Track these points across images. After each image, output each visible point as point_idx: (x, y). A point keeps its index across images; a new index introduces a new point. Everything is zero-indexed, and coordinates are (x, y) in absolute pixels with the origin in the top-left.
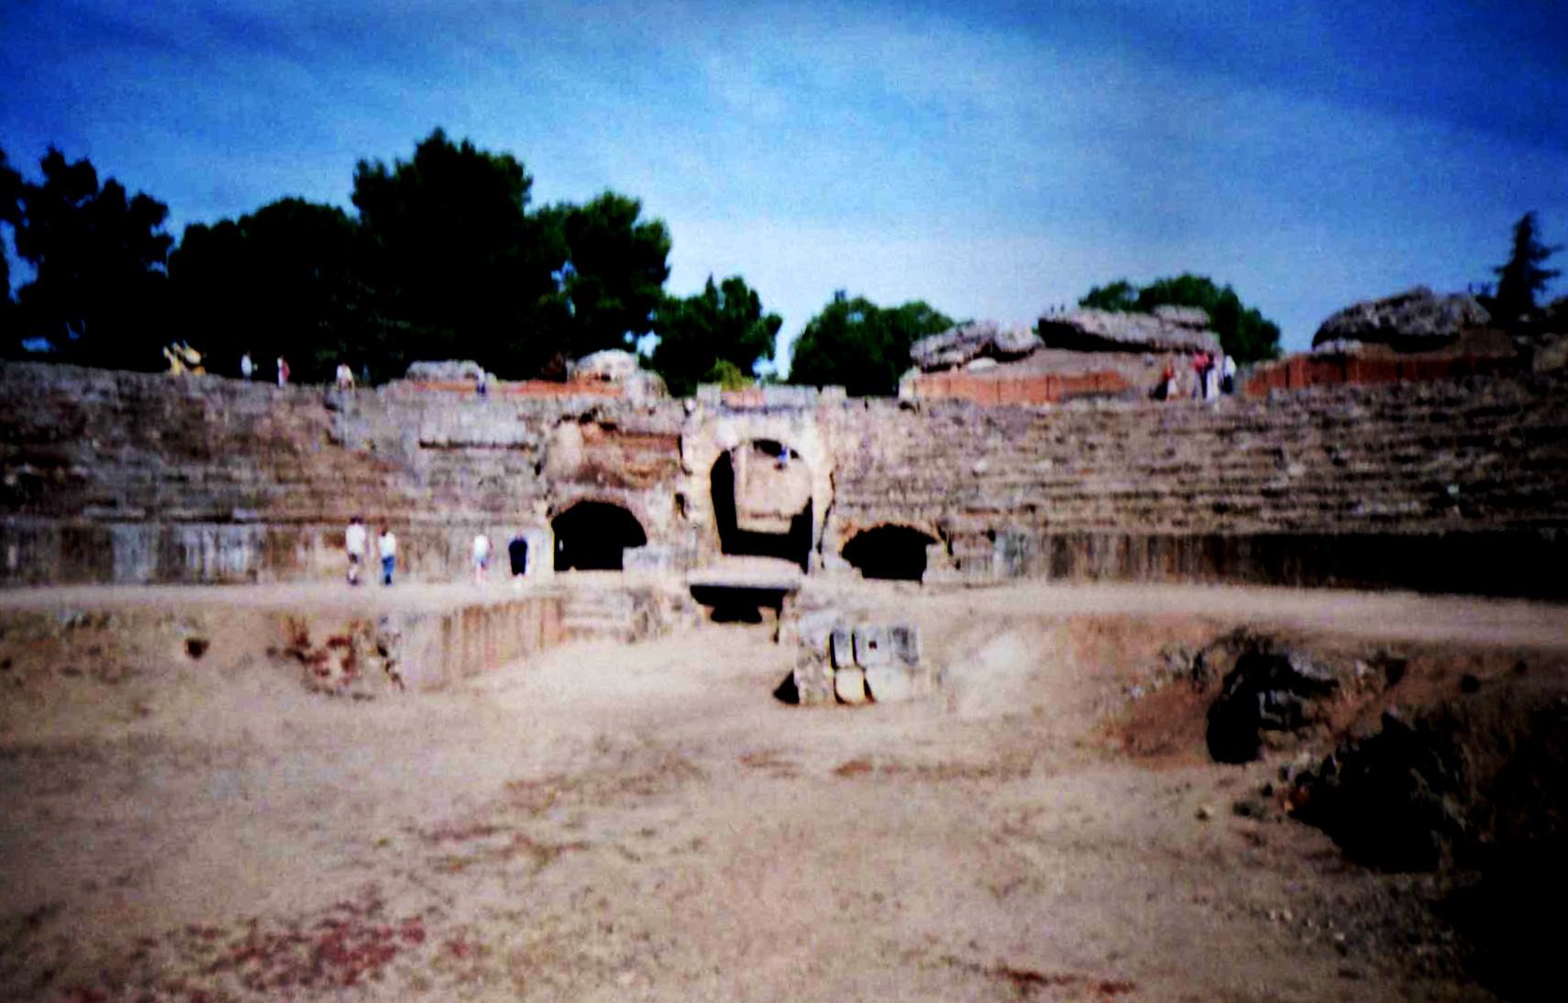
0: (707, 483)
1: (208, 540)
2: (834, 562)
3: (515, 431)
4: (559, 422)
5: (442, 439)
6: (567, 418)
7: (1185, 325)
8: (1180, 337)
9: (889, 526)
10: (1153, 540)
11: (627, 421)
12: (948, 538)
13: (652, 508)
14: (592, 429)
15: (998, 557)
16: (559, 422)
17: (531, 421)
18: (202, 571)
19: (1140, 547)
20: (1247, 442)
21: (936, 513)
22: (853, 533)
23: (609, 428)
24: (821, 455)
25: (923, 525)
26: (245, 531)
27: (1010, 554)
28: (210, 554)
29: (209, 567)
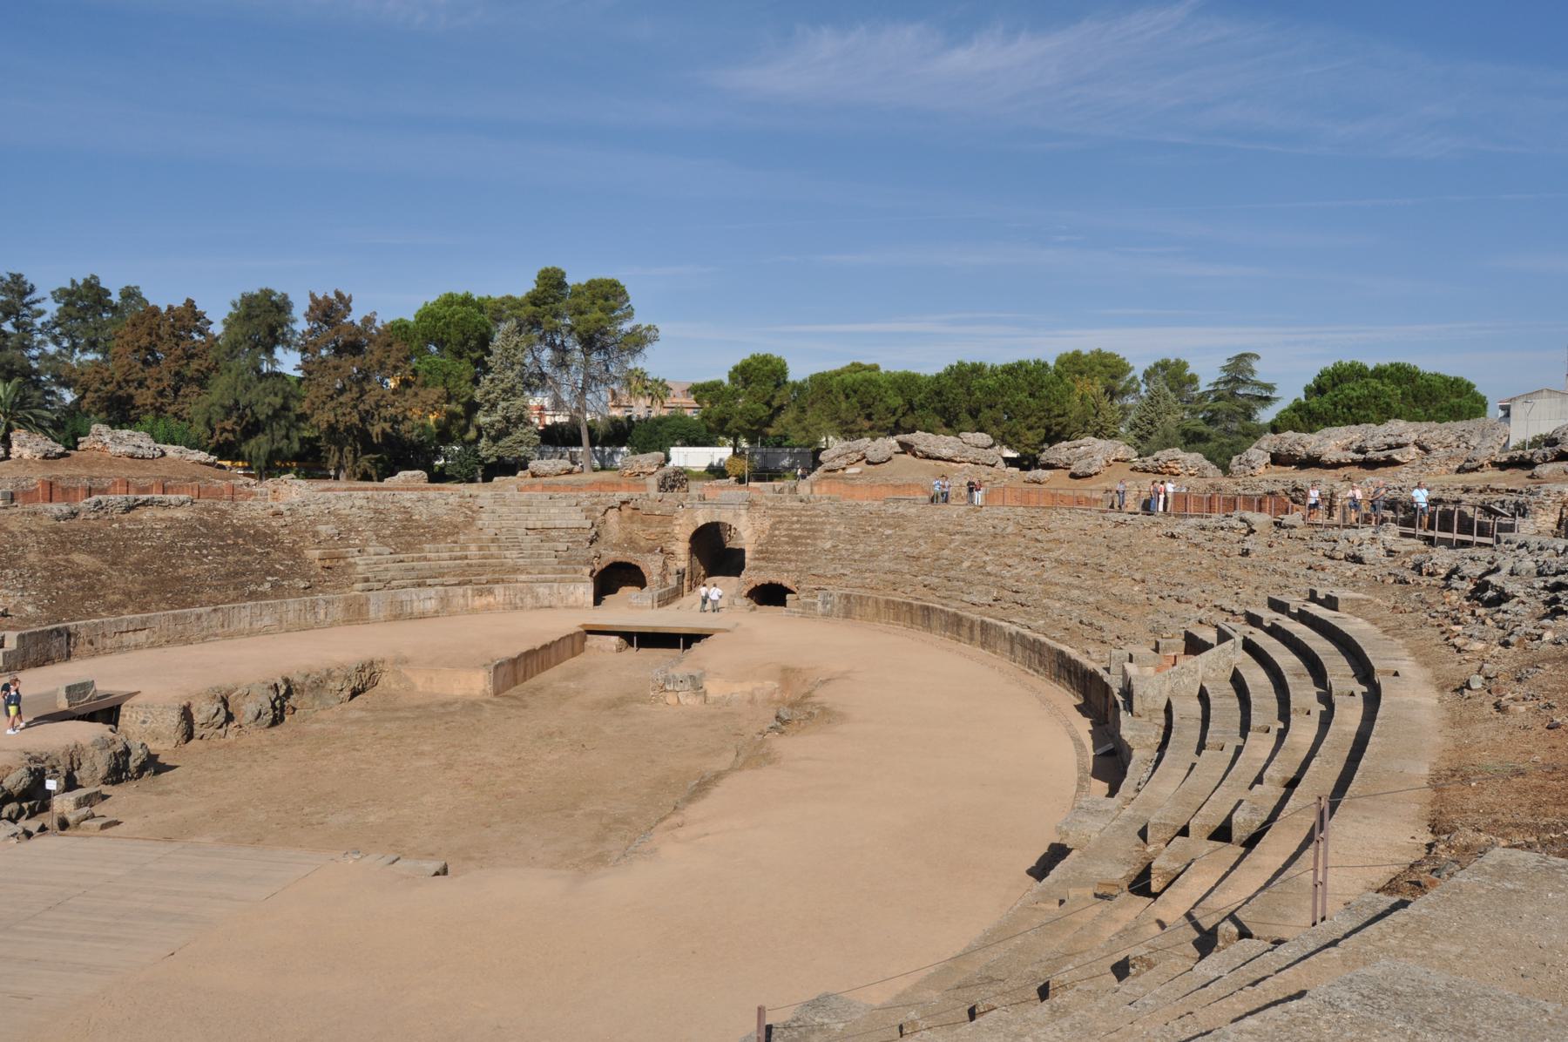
0: (687, 545)
1: (414, 597)
3: (577, 519)
4: (607, 510)
5: (539, 525)
6: (612, 507)
8: (972, 454)
9: (771, 584)
10: (887, 602)
11: (646, 506)
13: (651, 566)
14: (627, 511)
15: (820, 604)
16: (607, 510)
17: (589, 511)
18: (412, 613)
19: (882, 605)
21: (794, 576)
22: (753, 586)
24: (749, 531)
25: (787, 583)
26: (432, 592)
27: (825, 603)
28: (415, 604)
29: (415, 610)
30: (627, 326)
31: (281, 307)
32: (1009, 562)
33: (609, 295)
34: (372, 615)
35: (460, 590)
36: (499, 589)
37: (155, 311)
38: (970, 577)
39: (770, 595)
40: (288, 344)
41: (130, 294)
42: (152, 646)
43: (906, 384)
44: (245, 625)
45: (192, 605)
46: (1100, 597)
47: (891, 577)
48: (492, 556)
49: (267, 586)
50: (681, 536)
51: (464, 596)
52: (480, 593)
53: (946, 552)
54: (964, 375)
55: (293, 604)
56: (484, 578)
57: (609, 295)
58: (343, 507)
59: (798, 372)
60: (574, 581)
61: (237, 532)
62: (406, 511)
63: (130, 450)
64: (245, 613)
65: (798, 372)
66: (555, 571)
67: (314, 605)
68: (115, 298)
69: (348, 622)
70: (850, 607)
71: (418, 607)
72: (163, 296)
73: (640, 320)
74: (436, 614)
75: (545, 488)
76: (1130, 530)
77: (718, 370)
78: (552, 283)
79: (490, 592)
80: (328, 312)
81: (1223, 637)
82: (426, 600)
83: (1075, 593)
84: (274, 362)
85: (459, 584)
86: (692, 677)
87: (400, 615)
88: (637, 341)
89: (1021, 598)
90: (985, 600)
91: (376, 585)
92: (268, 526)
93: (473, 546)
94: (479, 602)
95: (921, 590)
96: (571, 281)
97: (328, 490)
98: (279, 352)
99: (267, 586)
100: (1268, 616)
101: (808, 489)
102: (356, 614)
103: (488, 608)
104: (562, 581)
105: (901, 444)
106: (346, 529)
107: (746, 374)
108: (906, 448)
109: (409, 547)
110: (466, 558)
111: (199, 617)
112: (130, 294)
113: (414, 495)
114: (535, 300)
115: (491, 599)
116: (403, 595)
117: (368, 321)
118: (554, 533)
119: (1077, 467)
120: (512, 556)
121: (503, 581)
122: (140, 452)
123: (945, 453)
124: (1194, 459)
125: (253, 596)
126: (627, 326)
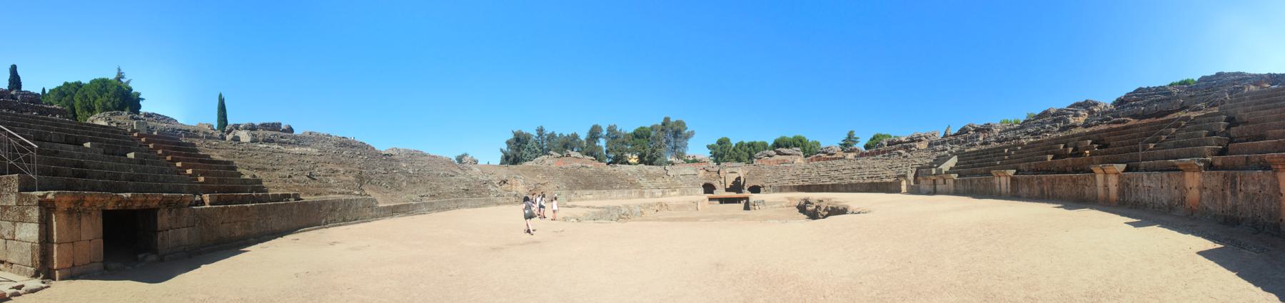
2: (746, 191)
3: (693, 172)
8: (796, 153)
12: (763, 187)
17: (696, 170)
20: (807, 170)
23: (707, 171)
33: (679, 123)
35: (667, 190)
36: (678, 190)
40: (601, 137)
42: (593, 199)
49: (618, 187)
52: (673, 191)
55: (626, 191)
59: (734, 142)
65: (734, 142)
67: (631, 193)
68: (558, 136)
69: (639, 198)
74: (662, 196)
78: (667, 120)
80: (611, 129)
84: (599, 142)
86: (763, 201)
94: (672, 193)
96: (671, 120)
98: (601, 139)
102: (642, 195)
103: (675, 196)
106: (634, 174)
107: (721, 142)
108: (779, 153)
115: (675, 193)
116: (653, 191)
117: (621, 130)
126: (686, 131)
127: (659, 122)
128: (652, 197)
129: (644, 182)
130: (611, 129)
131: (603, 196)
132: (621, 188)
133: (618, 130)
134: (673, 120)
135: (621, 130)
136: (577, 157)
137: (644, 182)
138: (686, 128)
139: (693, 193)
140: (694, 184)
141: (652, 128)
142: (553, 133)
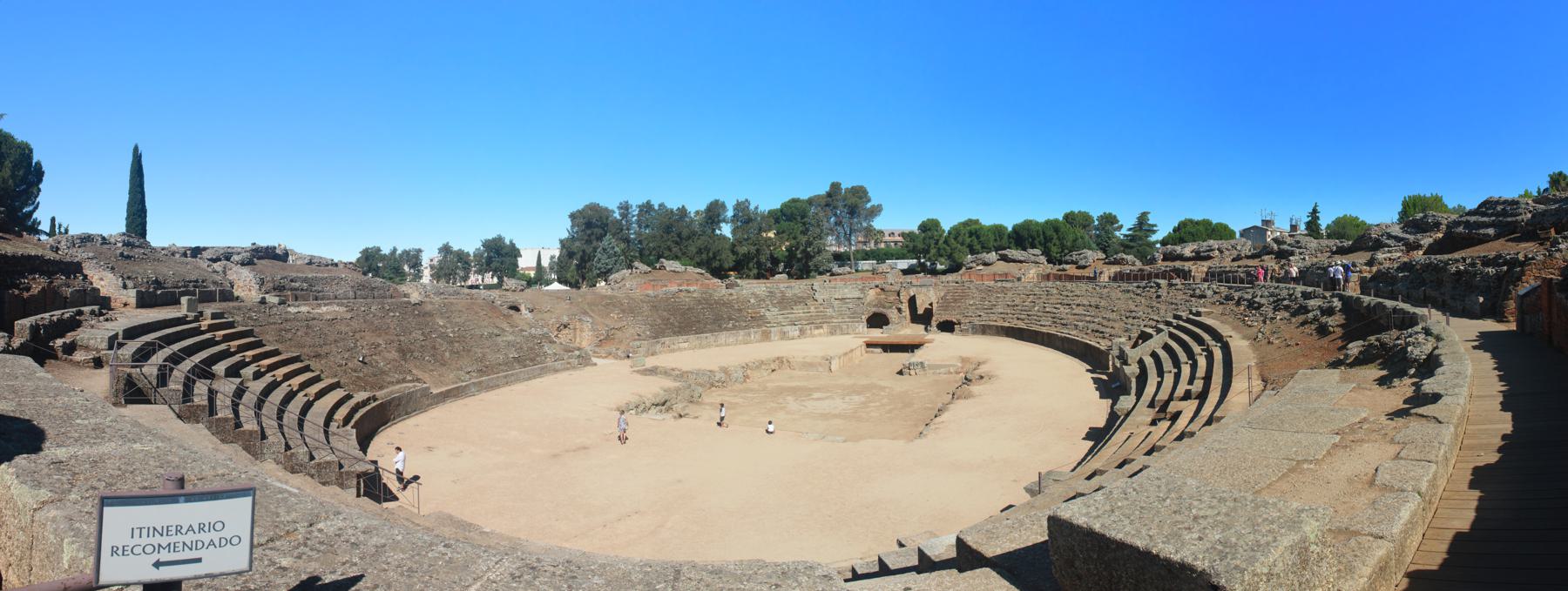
3: (857, 294)
7: (1034, 255)
8: (1033, 258)
12: (959, 324)
13: (892, 314)
17: (862, 290)
23: (882, 289)
30: (869, 205)
31: (723, 206)
32: (1057, 306)
33: (860, 193)
34: (772, 338)
35: (808, 327)
36: (825, 326)
37: (672, 211)
38: (1039, 314)
39: (947, 327)
40: (724, 221)
41: (661, 205)
42: (690, 349)
43: (998, 230)
44: (723, 341)
45: (702, 333)
46: (1100, 319)
47: (1002, 316)
48: (821, 312)
49: (731, 325)
50: (904, 301)
51: (811, 329)
52: (817, 328)
53: (1026, 303)
54: (1027, 225)
56: (818, 321)
57: (860, 193)
58: (757, 291)
59: (946, 225)
60: (857, 322)
61: (716, 303)
62: (782, 292)
63: (673, 269)
64: (723, 337)
65: (946, 225)
66: (849, 317)
67: (749, 334)
68: (656, 207)
70: (984, 330)
71: (791, 334)
72: (673, 204)
73: (874, 202)
75: (842, 280)
76: (1108, 289)
77: (913, 226)
78: (835, 187)
79: (821, 327)
80: (741, 207)
81: (1159, 331)
82: (793, 331)
83: (1088, 319)
85: (808, 324)
86: (922, 363)
87: (784, 336)
88: (876, 211)
89: (1065, 322)
90: (1047, 323)
91: (775, 325)
92: (728, 300)
93: (812, 308)
94: (816, 332)
95: (1016, 322)
96: (843, 187)
97: (749, 284)
98: (723, 225)
99: (731, 325)
100: (1175, 322)
101: (960, 278)
102: (766, 336)
103: (820, 335)
104: (852, 322)
105: (1000, 255)
106: (760, 300)
108: (1004, 258)
109: (785, 308)
110: (809, 312)
111: (706, 338)
112: (661, 205)
113: (786, 285)
114: (829, 195)
115: (821, 331)
116: (785, 329)
117: (757, 208)
118: (848, 301)
119: (1082, 263)
120: (829, 311)
121: (827, 322)
122: (677, 270)
123: (1022, 259)
124: (1130, 258)
125: (726, 329)
126: (869, 205)
127: (822, 189)
128: (782, 339)
129: (772, 313)
130: (741, 207)
131: (704, 342)
132: (734, 327)
133: (752, 207)
134: (846, 185)
135: (757, 208)
136: (674, 271)
137: (772, 313)
138: (869, 201)
139: (850, 331)
140: (854, 316)
141: (810, 202)
142: (648, 202)
